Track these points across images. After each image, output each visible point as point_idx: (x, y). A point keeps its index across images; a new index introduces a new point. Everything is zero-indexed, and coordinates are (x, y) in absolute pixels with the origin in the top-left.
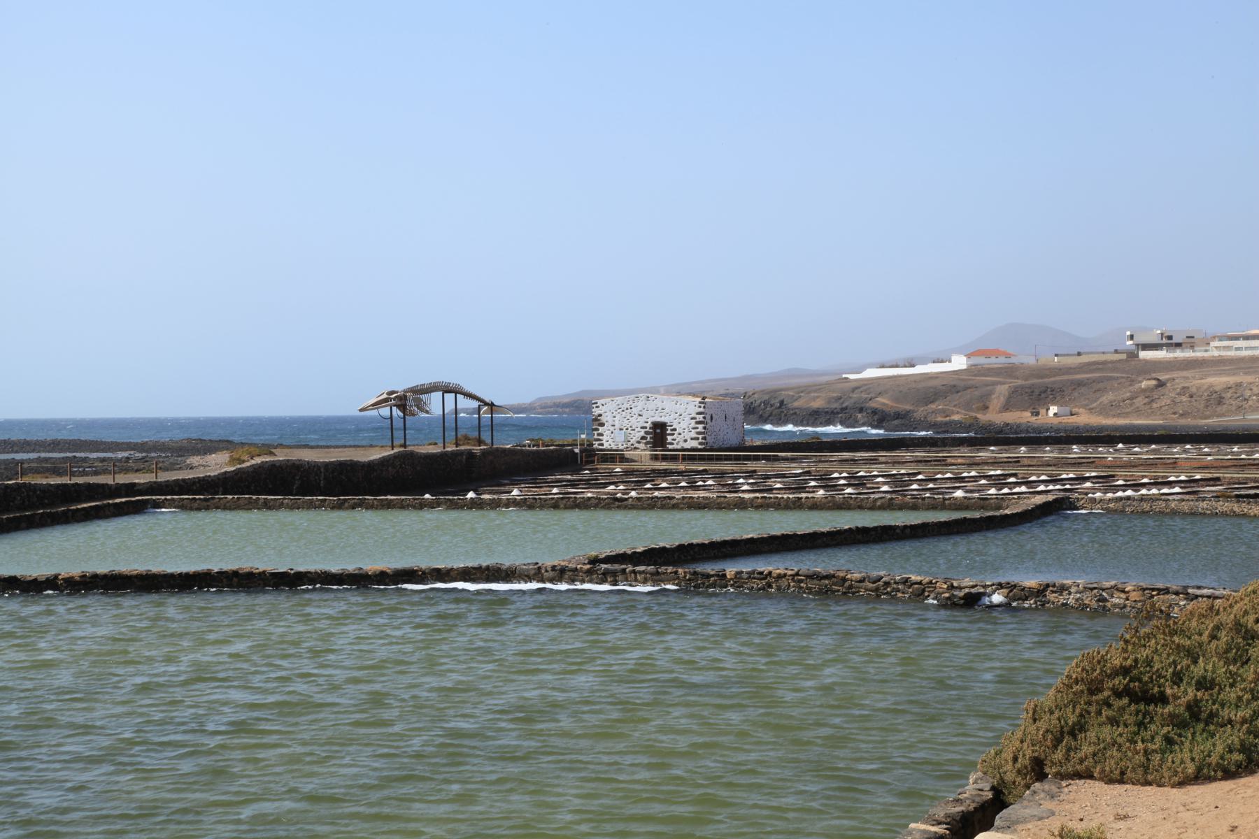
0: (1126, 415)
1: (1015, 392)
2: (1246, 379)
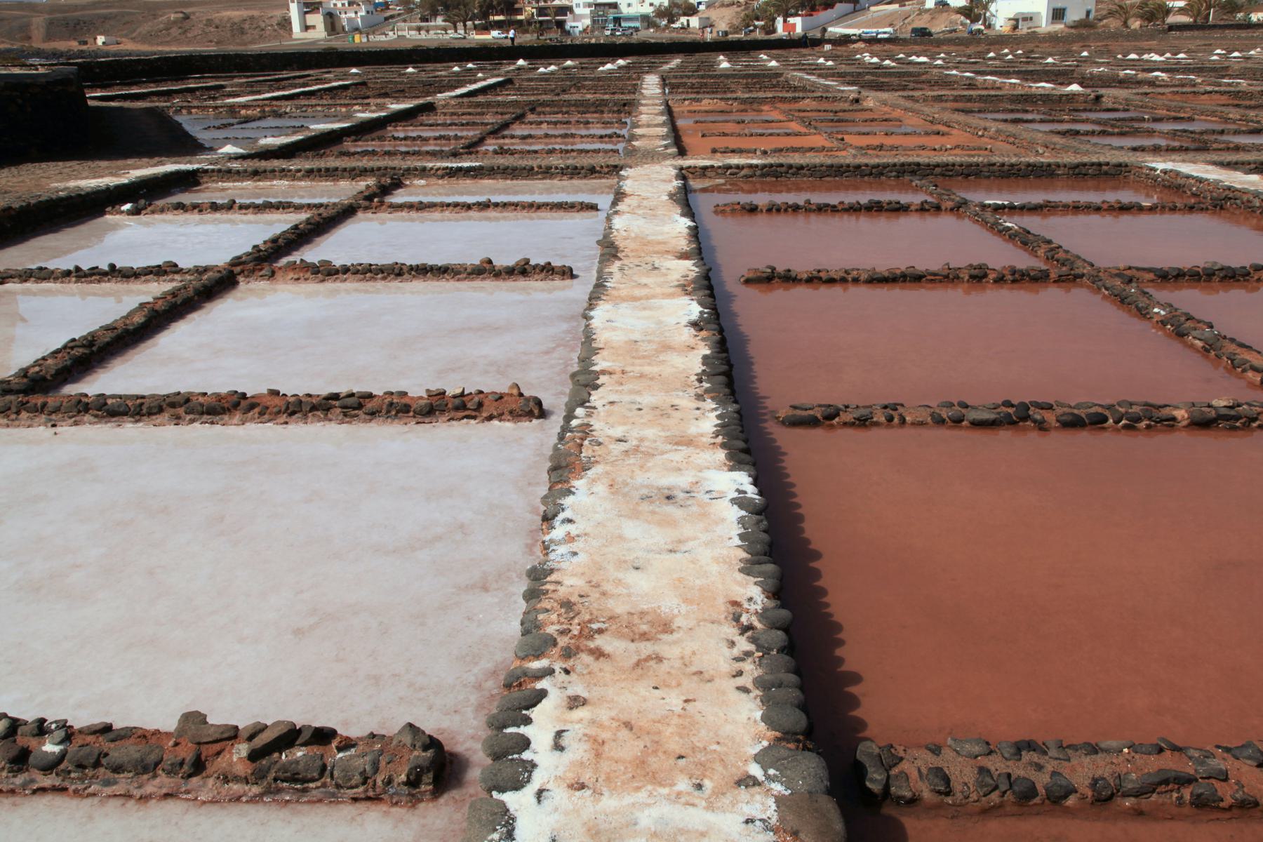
0: (168, 43)
1: (51, 23)
2: (256, 13)
